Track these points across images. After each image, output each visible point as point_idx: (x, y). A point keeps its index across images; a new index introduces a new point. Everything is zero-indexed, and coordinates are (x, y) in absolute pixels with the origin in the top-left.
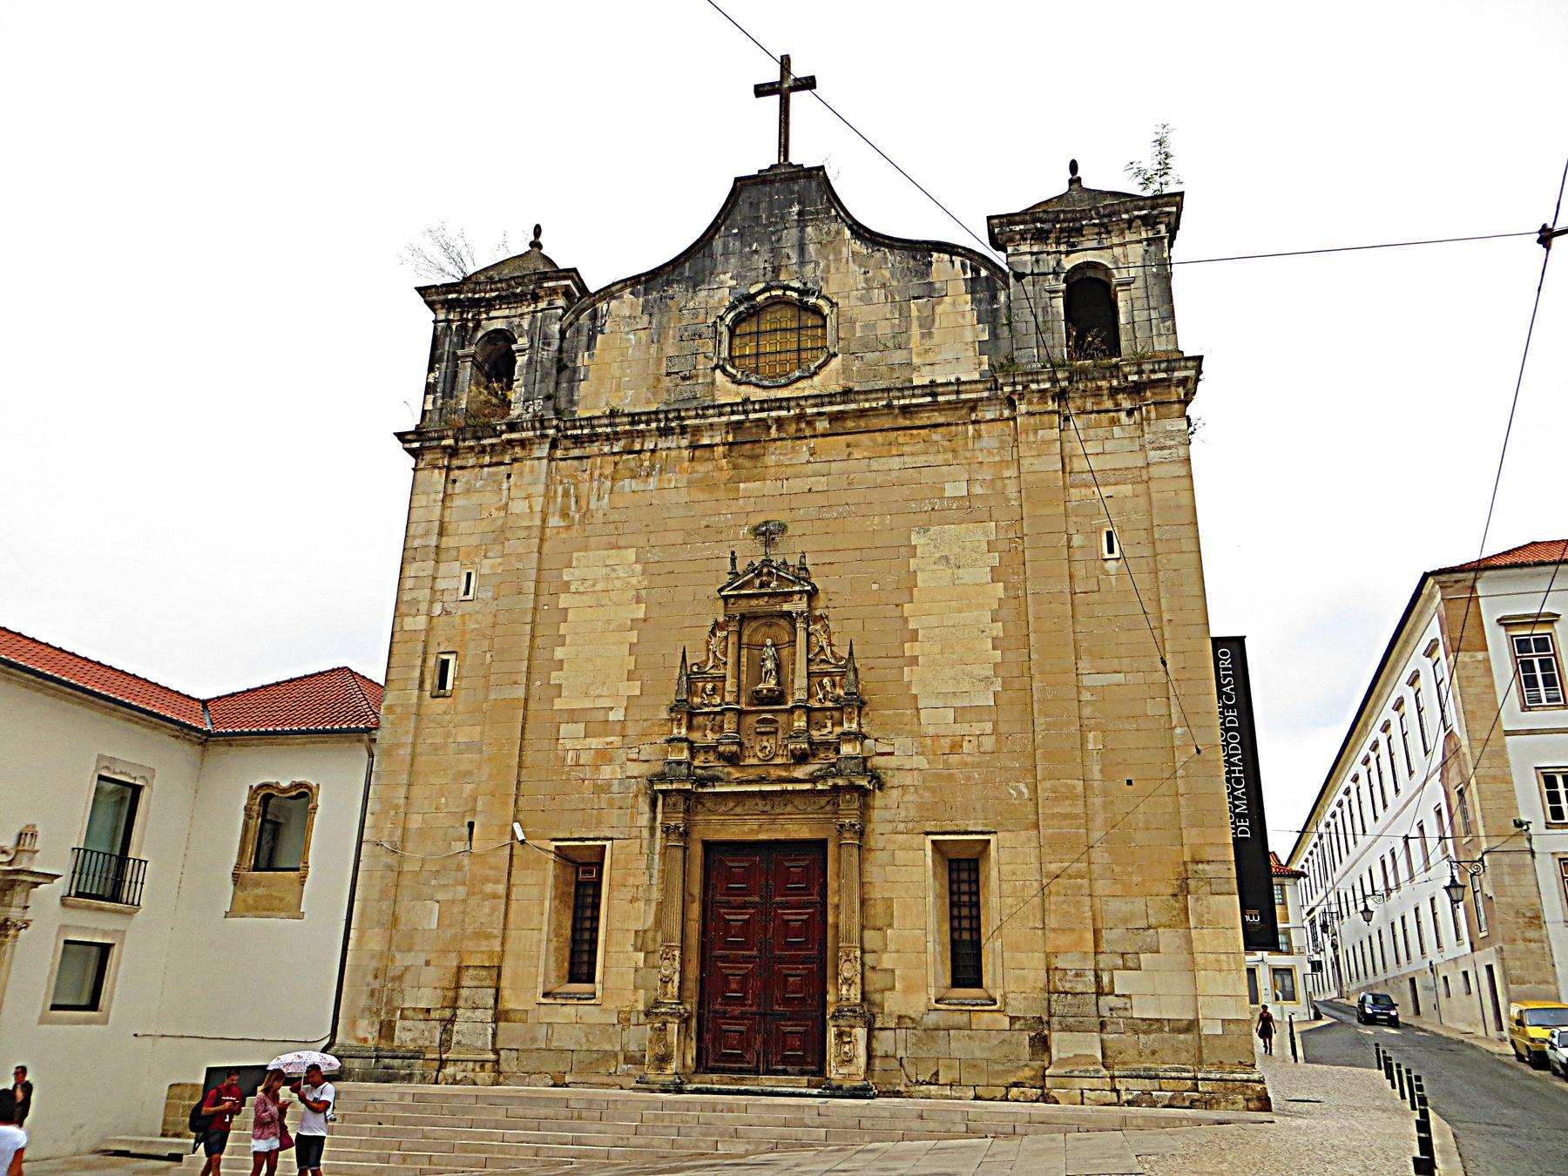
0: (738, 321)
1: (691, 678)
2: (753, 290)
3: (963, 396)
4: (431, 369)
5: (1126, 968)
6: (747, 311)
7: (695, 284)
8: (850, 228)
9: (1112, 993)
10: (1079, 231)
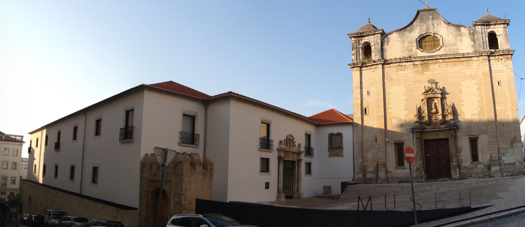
2: (424, 33)
7: (410, 31)
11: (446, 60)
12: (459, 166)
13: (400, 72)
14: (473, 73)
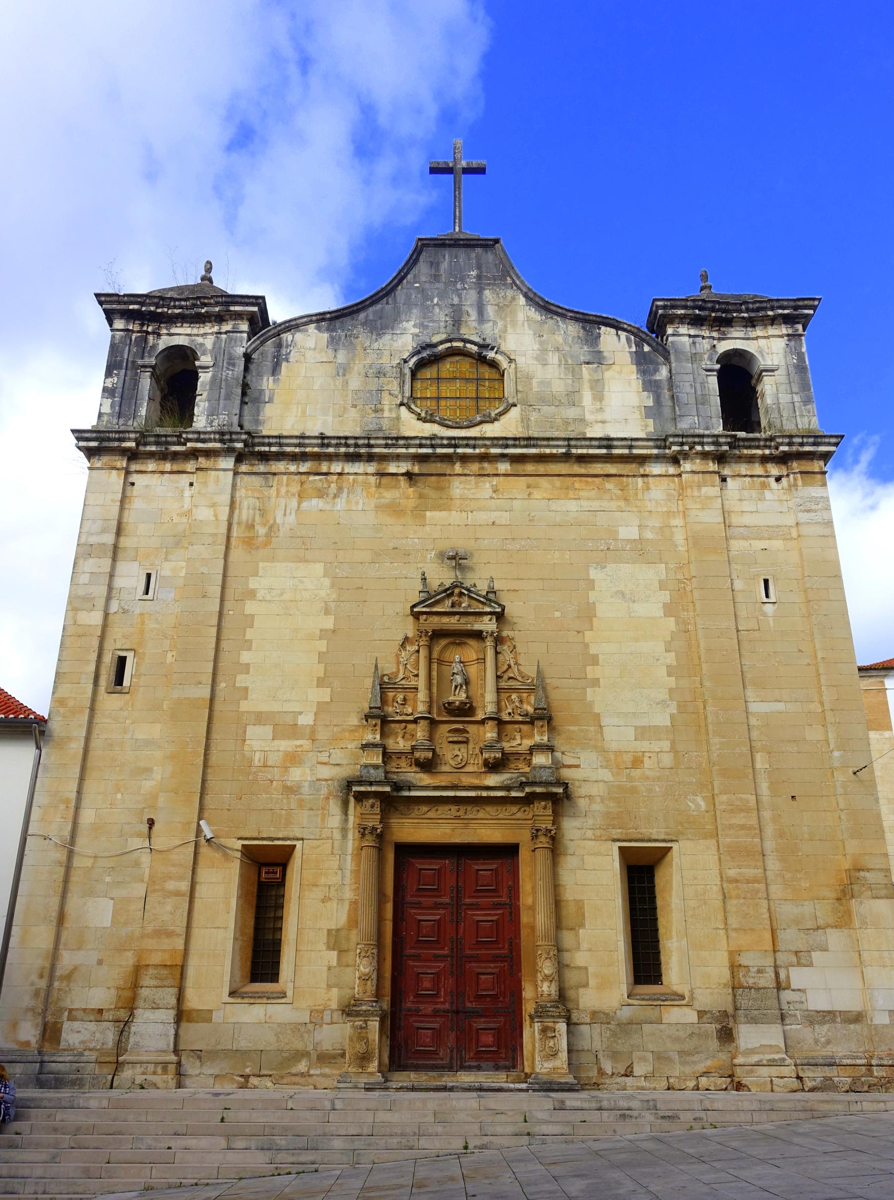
0: (422, 364)
1: (384, 686)
2: (436, 339)
3: (635, 451)
4: (109, 373)
5: (799, 964)
6: (427, 359)
7: (379, 328)
8: (526, 296)
9: (788, 987)
10: (729, 323)
11: (530, 468)
12: (562, 1003)
13: (315, 503)
14: (649, 535)
